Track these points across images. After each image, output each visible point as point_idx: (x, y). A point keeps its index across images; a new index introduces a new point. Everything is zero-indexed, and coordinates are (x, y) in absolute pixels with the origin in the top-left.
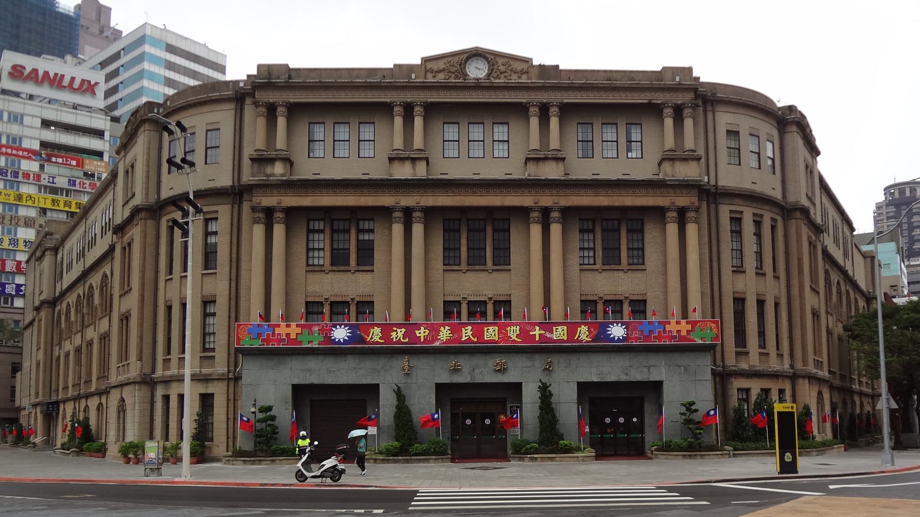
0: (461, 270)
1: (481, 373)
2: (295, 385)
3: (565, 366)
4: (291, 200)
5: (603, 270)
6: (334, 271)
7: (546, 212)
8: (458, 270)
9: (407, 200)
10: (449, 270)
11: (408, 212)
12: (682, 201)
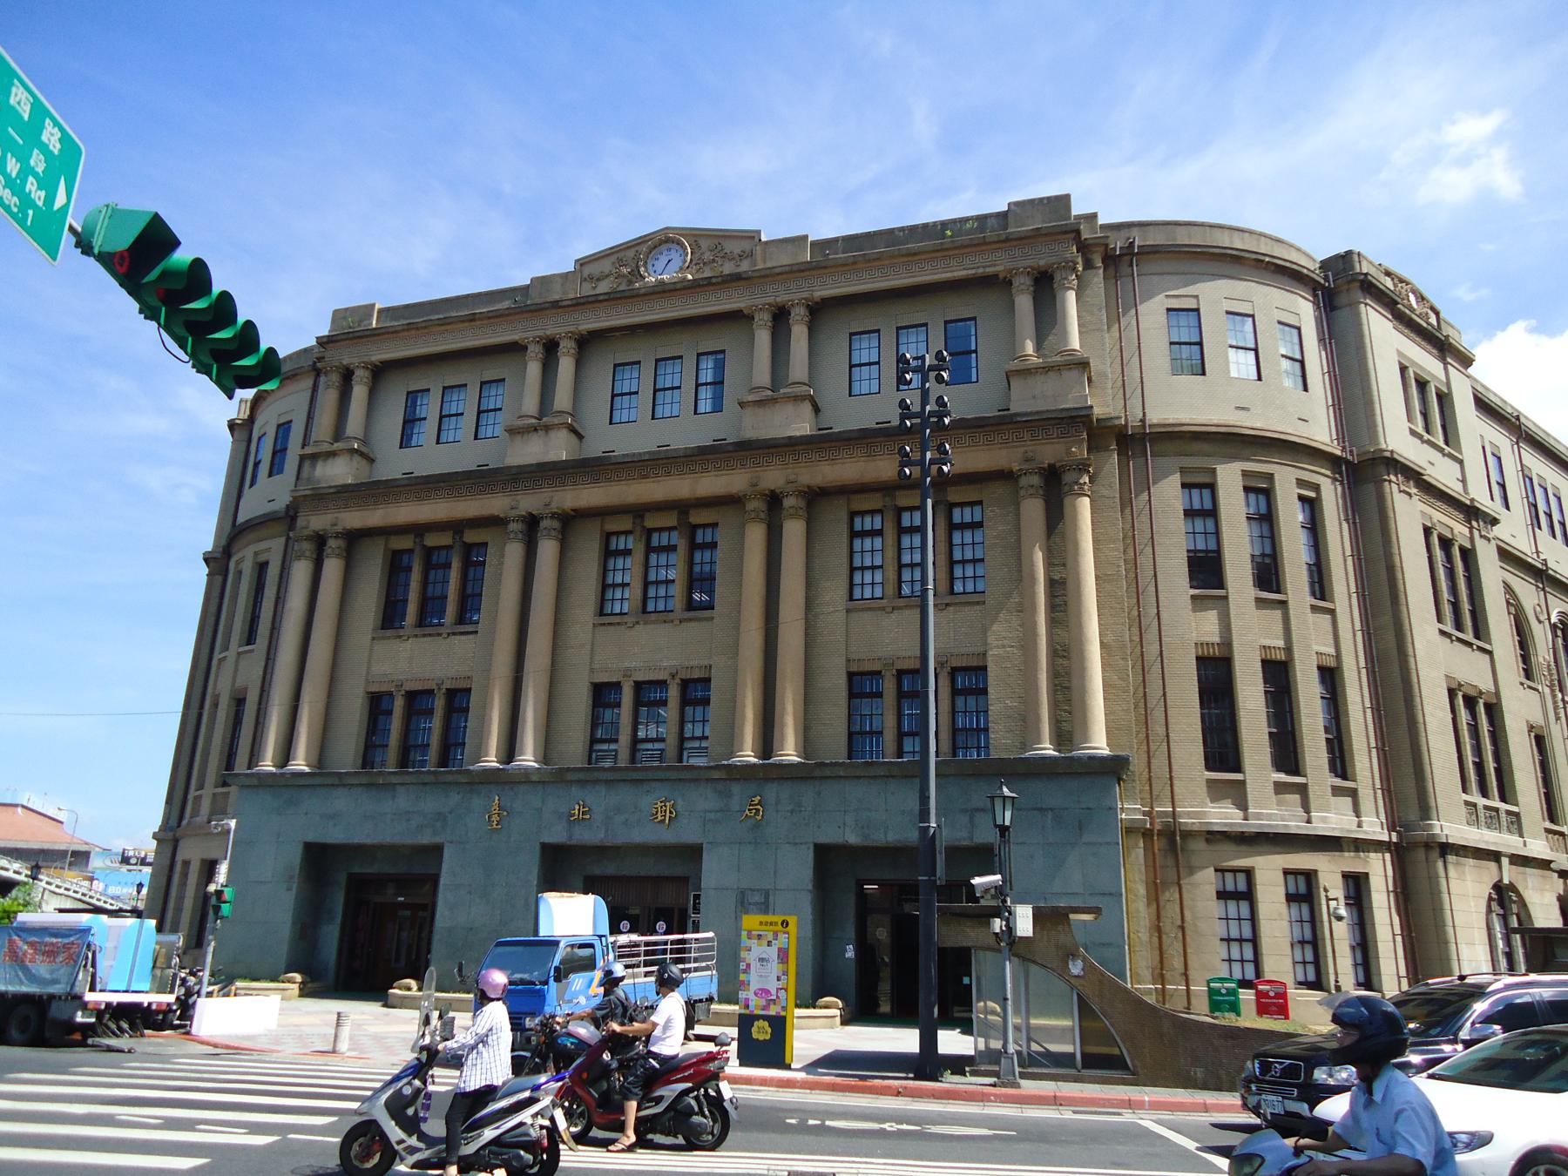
1: (626, 823)
2: (310, 843)
3: (790, 808)
4: (355, 519)
6: (416, 636)
7: (774, 500)
8: (618, 624)
9: (529, 502)
10: (604, 624)
11: (532, 523)
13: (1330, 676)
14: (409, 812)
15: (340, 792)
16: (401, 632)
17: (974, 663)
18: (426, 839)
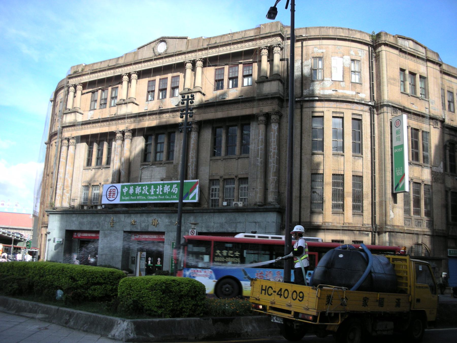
0: (149, 164)
5: (223, 159)
11: (123, 133)
12: (267, 108)
13: (358, 179)
14: (90, 222)
15: (74, 215)
16: (90, 167)
17: (245, 176)
18: (95, 229)
